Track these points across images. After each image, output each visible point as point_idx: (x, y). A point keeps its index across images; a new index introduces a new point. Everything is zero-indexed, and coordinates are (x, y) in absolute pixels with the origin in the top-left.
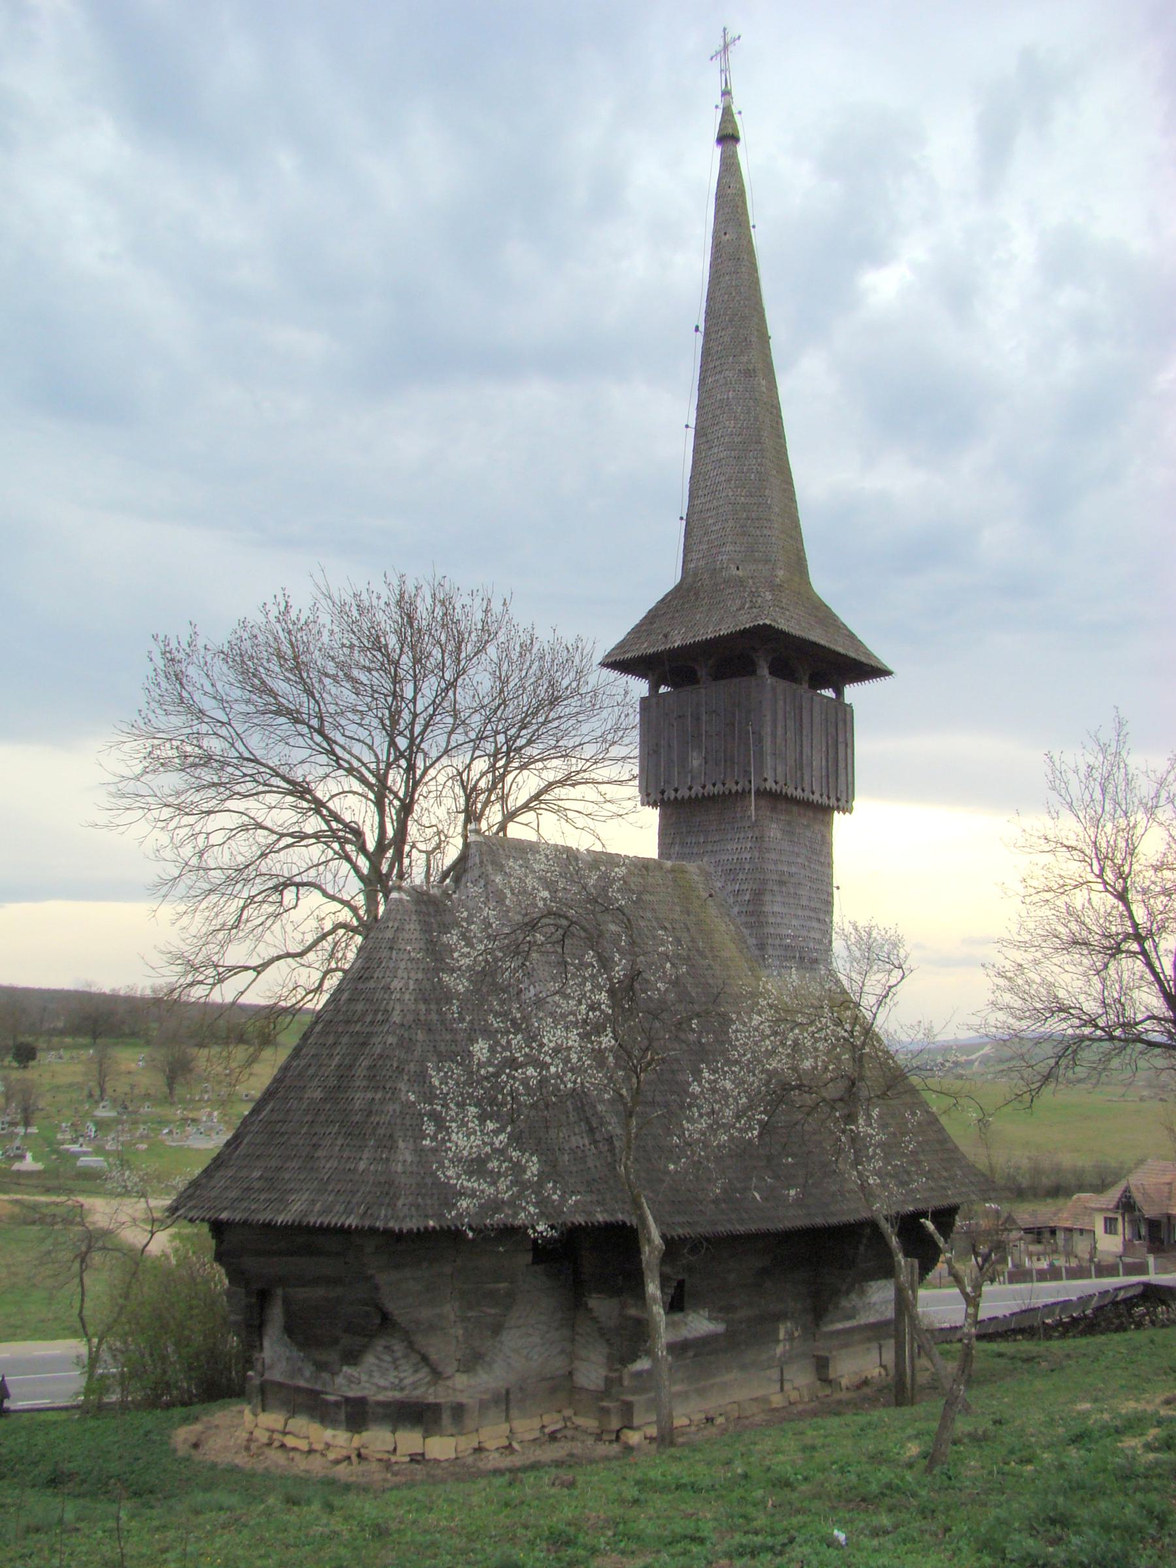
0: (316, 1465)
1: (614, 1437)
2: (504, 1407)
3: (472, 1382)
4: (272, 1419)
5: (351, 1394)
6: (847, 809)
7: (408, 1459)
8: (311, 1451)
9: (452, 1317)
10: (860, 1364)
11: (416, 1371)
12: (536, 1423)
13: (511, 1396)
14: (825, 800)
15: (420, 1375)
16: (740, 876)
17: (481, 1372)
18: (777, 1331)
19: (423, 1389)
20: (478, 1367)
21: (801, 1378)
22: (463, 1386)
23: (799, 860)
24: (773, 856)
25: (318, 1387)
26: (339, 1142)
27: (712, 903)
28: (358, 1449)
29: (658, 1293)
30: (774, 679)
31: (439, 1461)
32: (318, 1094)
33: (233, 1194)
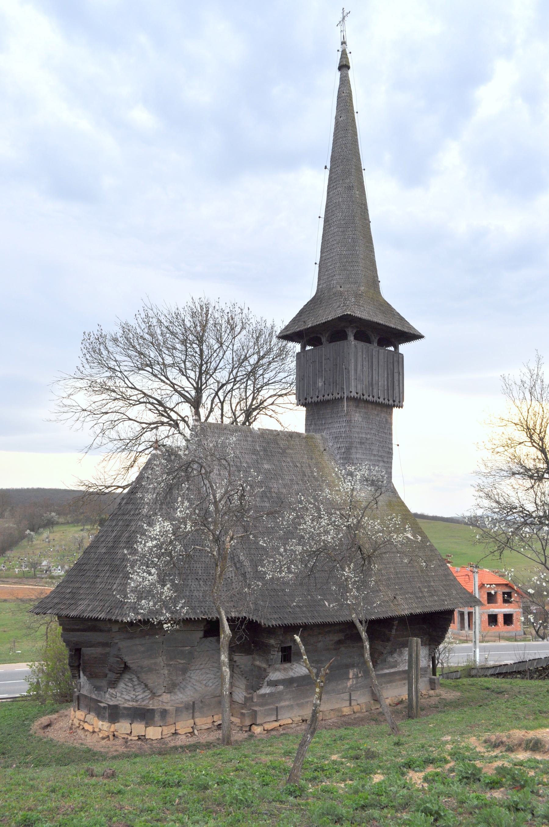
0: (91, 741)
1: (247, 729)
2: (192, 711)
3: (173, 698)
4: (80, 714)
5: (111, 703)
6: (400, 406)
7: (137, 738)
8: (94, 732)
9: (162, 664)
10: (394, 693)
11: (144, 692)
12: (209, 720)
13: (196, 705)
14: (386, 401)
15: (146, 694)
16: (340, 440)
17: (178, 693)
18: (349, 673)
20: (176, 690)
21: (362, 700)
22: (167, 701)
23: (372, 432)
24: (357, 430)
25: (99, 699)
26: (107, 575)
27: (325, 454)
29: (226, 660)
30: (356, 342)
31: (152, 740)
32: (104, 550)
33: (56, 601)
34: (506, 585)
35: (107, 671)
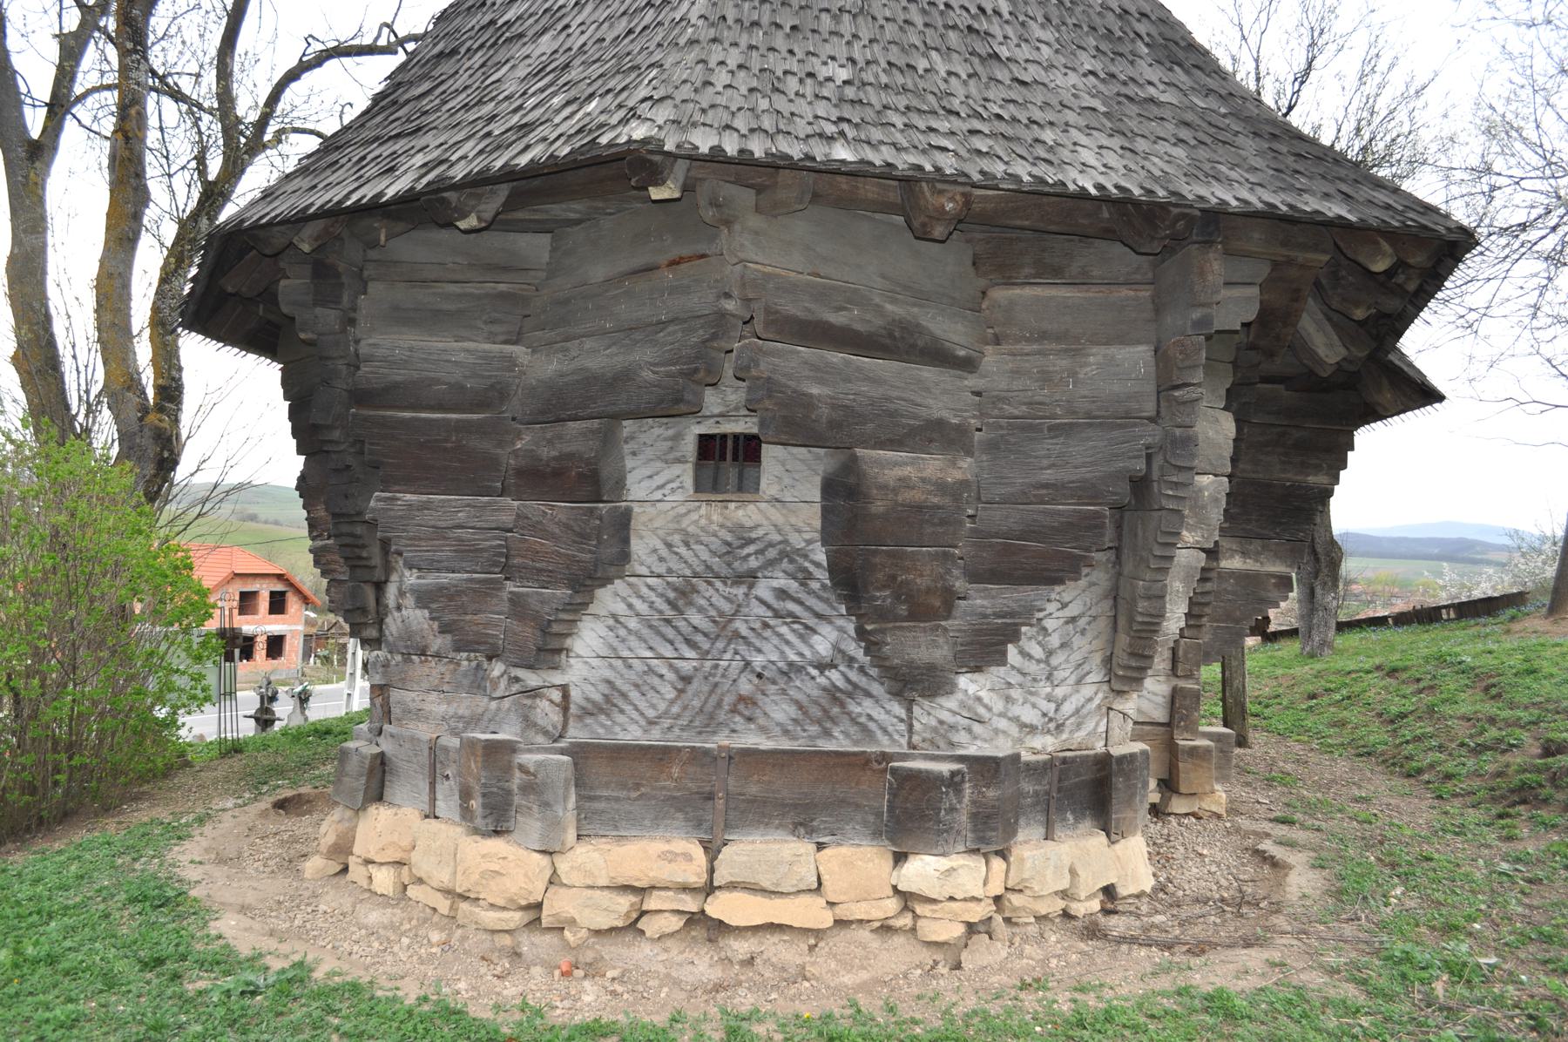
5: (972, 750)
11: (1079, 682)
15: (1087, 691)
19: (1089, 725)
25: (839, 742)
28: (997, 899)
34: (280, 577)
35: (960, 584)
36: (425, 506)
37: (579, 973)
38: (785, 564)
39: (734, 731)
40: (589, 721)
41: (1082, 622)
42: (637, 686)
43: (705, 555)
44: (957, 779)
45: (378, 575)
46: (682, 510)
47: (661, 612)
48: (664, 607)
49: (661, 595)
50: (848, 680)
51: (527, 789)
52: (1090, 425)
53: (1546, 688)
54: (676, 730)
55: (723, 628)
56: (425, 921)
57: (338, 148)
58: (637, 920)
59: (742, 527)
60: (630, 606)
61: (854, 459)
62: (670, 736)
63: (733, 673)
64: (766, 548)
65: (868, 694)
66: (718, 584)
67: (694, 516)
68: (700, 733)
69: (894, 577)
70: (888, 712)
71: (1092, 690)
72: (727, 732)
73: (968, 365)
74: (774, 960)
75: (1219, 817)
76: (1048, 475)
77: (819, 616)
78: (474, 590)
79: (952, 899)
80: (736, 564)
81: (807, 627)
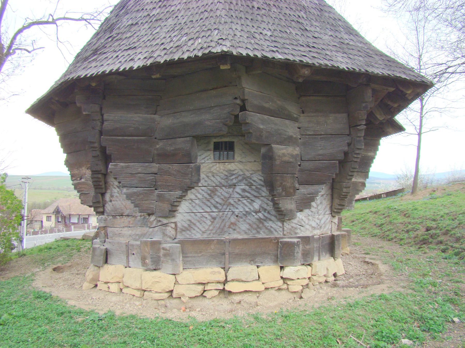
5: (301, 235)
19: (327, 227)
25: (262, 235)
28: (309, 278)
36: (127, 167)
37: (188, 310)
38: (244, 181)
39: (229, 234)
40: (184, 233)
41: (325, 196)
42: (199, 221)
43: (219, 179)
44: (298, 243)
45: (103, 191)
46: (211, 165)
47: (206, 198)
48: (206, 195)
49: (206, 192)
50: (265, 216)
51: (165, 255)
52: (332, 137)
53: (421, 213)
54: (212, 234)
55: (226, 202)
56: (131, 299)
57: (105, 53)
58: (203, 293)
59: (230, 170)
60: (196, 196)
61: (272, 147)
62: (210, 236)
63: (229, 216)
64: (238, 176)
65: (271, 220)
66: (224, 188)
67: (215, 167)
68: (219, 235)
69: (282, 183)
70: (277, 225)
71: (328, 217)
72: (227, 234)
73: (295, 120)
74: (247, 301)
75: (348, 254)
76: (321, 152)
77: (255, 197)
78: (146, 193)
79: (298, 279)
80: (229, 182)
81: (252, 200)
